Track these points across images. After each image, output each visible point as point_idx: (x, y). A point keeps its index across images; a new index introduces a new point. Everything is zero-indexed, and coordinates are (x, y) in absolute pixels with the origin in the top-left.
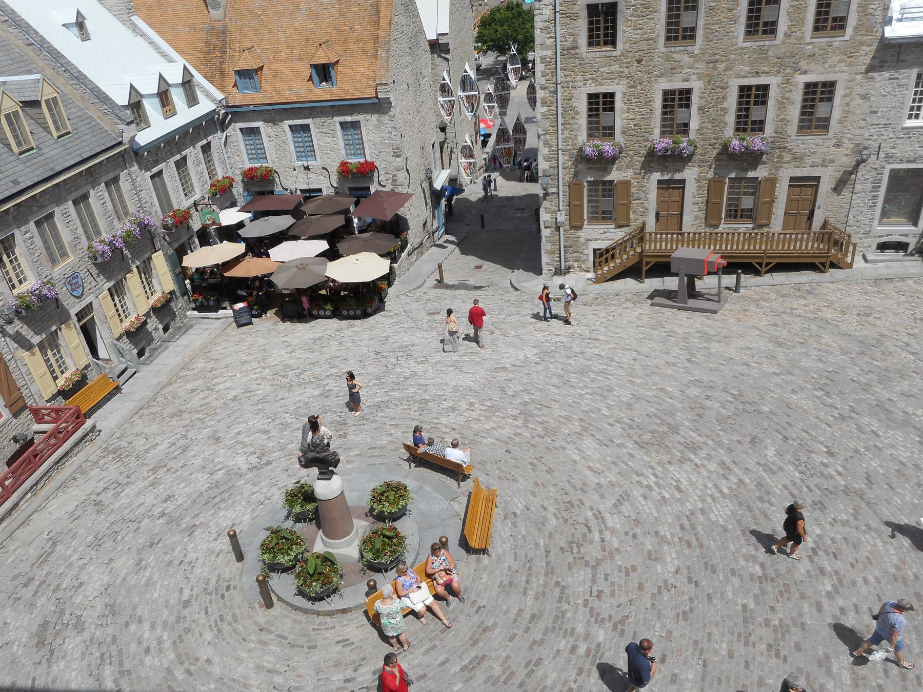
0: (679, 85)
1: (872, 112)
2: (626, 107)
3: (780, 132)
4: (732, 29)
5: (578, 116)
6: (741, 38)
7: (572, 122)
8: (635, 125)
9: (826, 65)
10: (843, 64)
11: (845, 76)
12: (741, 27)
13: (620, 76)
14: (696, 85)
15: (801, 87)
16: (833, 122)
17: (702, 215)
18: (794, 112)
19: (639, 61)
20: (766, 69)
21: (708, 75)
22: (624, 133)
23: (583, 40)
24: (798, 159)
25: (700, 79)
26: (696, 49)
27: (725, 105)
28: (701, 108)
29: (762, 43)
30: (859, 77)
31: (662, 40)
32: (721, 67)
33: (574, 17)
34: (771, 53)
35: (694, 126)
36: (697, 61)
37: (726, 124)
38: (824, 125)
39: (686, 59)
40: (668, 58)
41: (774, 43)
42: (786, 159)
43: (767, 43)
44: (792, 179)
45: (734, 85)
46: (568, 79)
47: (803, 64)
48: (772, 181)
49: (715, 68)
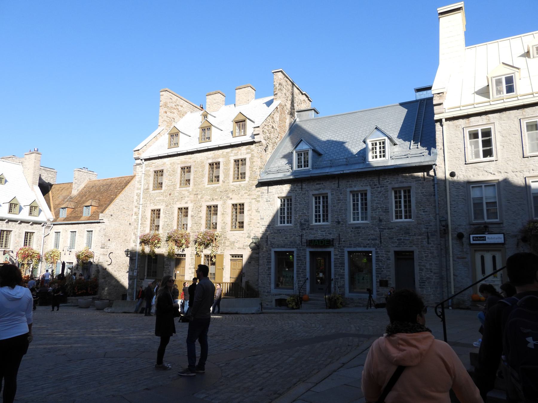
0: (183, 205)
1: (261, 219)
3: (223, 228)
6: (207, 183)
7: (144, 223)
8: (167, 225)
9: (240, 196)
10: (247, 195)
11: (249, 201)
12: (206, 179)
13: (163, 201)
14: (190, 206)
16: (245, 225)
18: (228, 219)
19: (170, 194)
20: (216, 197)
21: (195, 201)
22: (163, 228)
25: (191, 202)
29: (214, 185)
30: (254, 200)
32: (199, 197)
34: (218, 190)
35: (189, 226)
36: (190, 194)
38: (241, 225)
39: (186, 193)
40: (180, 193)
42: (227, 245)
43: (216, 185)
44: (233, 256)
47: (230, 195)
48: (222, 256)
49: (197, 197)
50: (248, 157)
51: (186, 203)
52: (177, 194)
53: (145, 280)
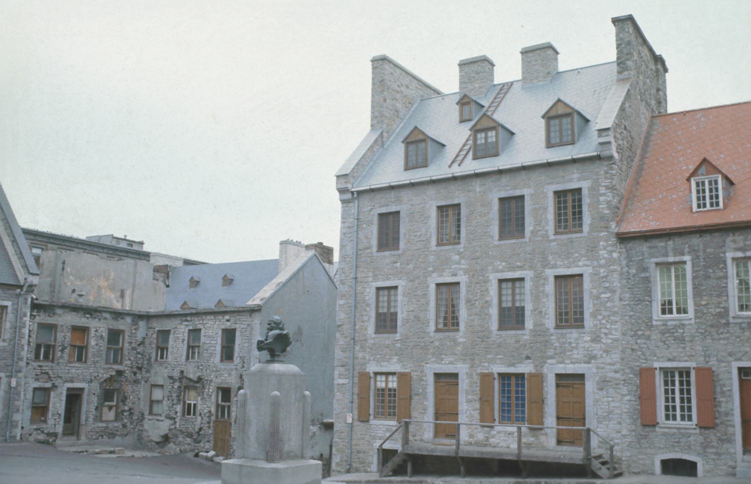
2: (406, 299)
4: (489, 230)
5: (368, 309)
12: (495, 230)
14: (462, 279)
15: (552, 279)
17: (476, 415)
23: (374, 242)
24: (562, 354)
26: (461, 247)
27: (488, 299)
28: (468, 301)
31: (434, 241)
33: (370, 223)
36: (463, 258)
37: (490, 316)
41: (524, 240)
45: (493, 278)
46: (363, 275)
48: (538, 378)
50: (585, 185)
51: (455, 275)
52: (432, 258)
53: (373, 422)
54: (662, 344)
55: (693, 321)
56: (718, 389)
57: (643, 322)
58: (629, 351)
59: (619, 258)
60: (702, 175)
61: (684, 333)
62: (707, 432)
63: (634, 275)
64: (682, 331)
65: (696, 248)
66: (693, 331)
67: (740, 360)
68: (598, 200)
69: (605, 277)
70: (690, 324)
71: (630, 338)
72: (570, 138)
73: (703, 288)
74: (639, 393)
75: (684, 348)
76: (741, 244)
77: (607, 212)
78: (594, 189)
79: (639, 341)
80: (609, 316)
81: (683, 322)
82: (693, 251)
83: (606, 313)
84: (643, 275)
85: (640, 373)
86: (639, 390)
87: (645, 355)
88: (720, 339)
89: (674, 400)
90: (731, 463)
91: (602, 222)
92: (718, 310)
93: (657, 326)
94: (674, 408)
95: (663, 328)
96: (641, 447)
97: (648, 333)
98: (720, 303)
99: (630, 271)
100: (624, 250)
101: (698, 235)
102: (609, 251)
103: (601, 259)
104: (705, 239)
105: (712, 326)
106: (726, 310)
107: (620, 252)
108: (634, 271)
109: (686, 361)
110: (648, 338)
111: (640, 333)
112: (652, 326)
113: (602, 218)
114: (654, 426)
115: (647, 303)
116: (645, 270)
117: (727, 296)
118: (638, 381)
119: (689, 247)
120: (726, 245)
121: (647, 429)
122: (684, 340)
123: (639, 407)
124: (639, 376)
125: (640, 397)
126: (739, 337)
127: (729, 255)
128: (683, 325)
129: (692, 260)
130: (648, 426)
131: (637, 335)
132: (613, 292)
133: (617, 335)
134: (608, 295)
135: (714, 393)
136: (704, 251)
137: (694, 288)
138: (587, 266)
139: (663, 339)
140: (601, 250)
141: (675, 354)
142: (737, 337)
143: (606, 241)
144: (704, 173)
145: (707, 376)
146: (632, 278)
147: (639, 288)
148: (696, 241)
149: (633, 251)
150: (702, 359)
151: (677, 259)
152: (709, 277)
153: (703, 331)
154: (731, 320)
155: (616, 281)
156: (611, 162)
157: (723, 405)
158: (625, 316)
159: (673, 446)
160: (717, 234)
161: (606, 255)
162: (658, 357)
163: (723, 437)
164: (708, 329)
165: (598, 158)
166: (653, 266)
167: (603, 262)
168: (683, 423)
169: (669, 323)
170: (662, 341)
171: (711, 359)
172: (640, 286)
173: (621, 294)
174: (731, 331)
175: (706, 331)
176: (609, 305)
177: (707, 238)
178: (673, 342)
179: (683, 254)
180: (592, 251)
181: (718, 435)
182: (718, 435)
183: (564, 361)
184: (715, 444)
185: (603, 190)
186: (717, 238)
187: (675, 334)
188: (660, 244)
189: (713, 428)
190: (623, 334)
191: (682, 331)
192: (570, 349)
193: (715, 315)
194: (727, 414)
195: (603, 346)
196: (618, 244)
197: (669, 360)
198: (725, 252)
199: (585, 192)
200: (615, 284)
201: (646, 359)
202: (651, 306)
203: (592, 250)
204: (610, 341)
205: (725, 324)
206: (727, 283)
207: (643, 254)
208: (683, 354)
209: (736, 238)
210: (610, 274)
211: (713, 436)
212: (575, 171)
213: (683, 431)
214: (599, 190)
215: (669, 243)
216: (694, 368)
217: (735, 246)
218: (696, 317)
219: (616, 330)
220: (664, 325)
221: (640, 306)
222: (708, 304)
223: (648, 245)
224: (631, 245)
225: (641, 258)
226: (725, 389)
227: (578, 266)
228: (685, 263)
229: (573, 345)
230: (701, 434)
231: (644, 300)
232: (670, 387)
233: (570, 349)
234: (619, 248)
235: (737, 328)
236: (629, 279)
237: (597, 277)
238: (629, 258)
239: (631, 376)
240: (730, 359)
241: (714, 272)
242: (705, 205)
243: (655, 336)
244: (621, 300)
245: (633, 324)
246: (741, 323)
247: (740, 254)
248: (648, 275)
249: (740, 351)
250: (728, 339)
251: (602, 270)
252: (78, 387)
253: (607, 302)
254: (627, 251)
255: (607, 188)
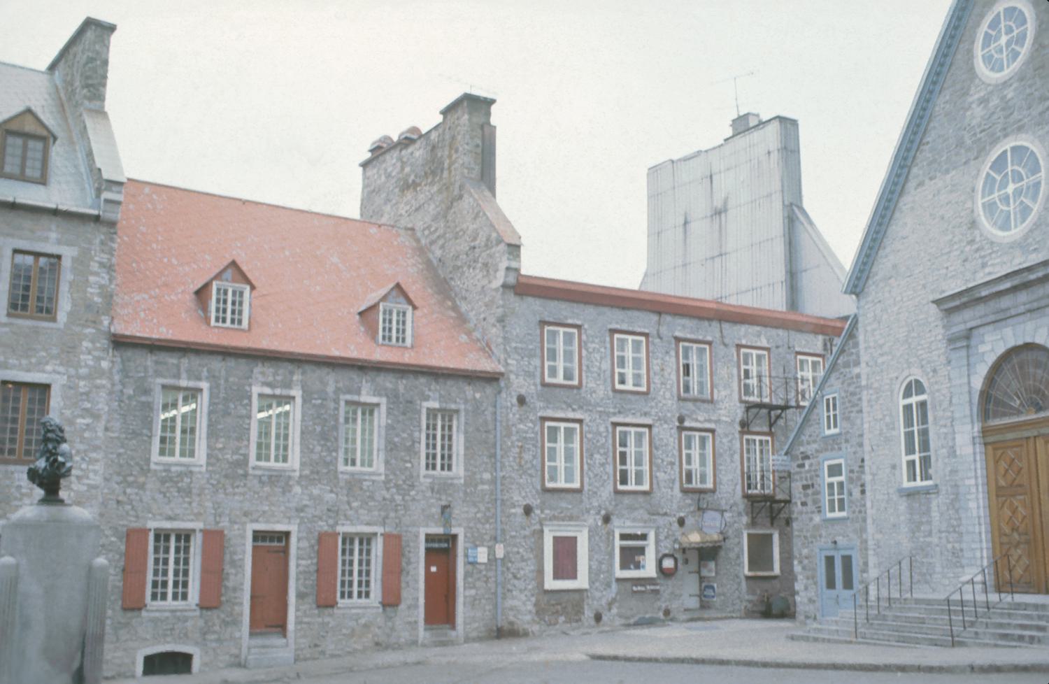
54: (161, 496)
55: (204, 469)
56: (227, 557)
57: (137, 464)
58: (113, 504)
59: (111, 369)
60: (227, 280)
61: (191, 482)
62: (209, 613)
63: (130, 398)
64: (189, 480)
65: (217, 374)
66: (204, 481)
67: (257, 521)
68: (87, 280)
69: (87, 394)
70: (200, 473)
71: (116, 486)
72: (37, 174)
73: (220, 427)
74: (122, 563)
75: (190, 503)
76: (271, 379)
77: (97, 299)
78: (81, 262)
79: (129, 491)
80: (85, 451)
81: (194, 469)
82: (212, 377)
83: (82, 447)
84: (143, 399)
85: (128, 535)
86: (123, 559)
87: (136, 511)
88: (234, 494)
89: (165, 573)
90: (234, 651)
91: (88, 312)
92: (235, 457)
93: (155, 471)
94: (165, 584)
95: (164, 474)
96: (118, 640)
97: (142, 479)
98: (239, 448)
99: (125, 391)
100: (119, 360)
101: (220, 358)
102: (93, 355)
103: (81, 367)
104: (229, 364)
105: (226, 476)
106: (246, 457)
107: (113, 362)
108: (131, 392)
109: (192, 520)
110: (142, 487)
111: (131, 479)
112: (149, 470)
113: (89, 307)
114: (140, 609)
115: (145, 438)
116: (147, 392)
117: (249, 440)
118: (123, 548)
119: (208, 371)
120: (254, 376)
121: (129, 614)
122: (190, 492)
123: (121, 584)
124: (124, 540)
125: (124, 570)
126: (258, 493)
127: (256, 390)
128: (191, 472)
129: (211, 389)
130: (132, 609)
131: (126, 481)
132: (96, 417)
133: (96, 479)
134: (88, 421)
135: (221, 561)
136: (227, 380)
137: (209, 426)
138: (59, 373)
139: (163, 490)
140: (84, 354)
141: (178, 511)
142: (255, 492)
143: (93, 342)
144: (230, 279)
145: (215, 541)
146: (127, 402)
147: (135, 416)
148: (217, 364)
149: (132, 364)
150: (211, 518)
151: (191, 384)
152: (229, 414)
153: (215, 482)
154: (251, 471)
155: (102, 403)
156: (112, 231)
157: (232, 577)
158: (112, 453)
159: (166, 635)
160: (243, 361)
161: (91, 363)
162: (154, 515)
163: (227, 619)
164: (223, 480)
165: (97, 219)
166: (158, 389)
167: (83, 371)
168: (176, 603)
169: (173, 469)
170: (161, 492)
171: (223, 519)
172: (137, 413)
173: (108, 421)
174: (249, 485)
175: (219, 482)
176: (87, 435)
177: (232, 363)
178: (176, 494)
179: (199, 379)
180: (68, 352)
181: (223, 616)
182: (223, 616)
183: (5, 514)
184: (217, 628)
185: (94, 267)
186: (354, 375)
187: (180, 485)
188: (172, 360)
189: (216, 608)
190: (106, 480)
191: (189, 480)
192: (18, 496)
193: (232, 463)
194: (235, 590)
195: (72, 494)
196: (111, 351)
197: (170, 518)
198: (250, 385)
199: (66, 263)
200: (100, 406)
201: (137, 517)
202: (150, 443)
203: (69, 351)
204: (85, 488)
205: (242, 475)
206: (249, 424)
207: (146, 368)
208: (188, 512)
209: (265, 369)
210: (94, 390)
211: (214, 615)
212: (53, 227)
213: (178, 614)
214: (89, 266)
215: (182, 360)
216: (201, 530)
217: (263, 380)
218: (208, 464)
219: (95, 472)
220: (165, 471)
221: (134, 442)
222: (224, 448)
223: (154, 358)
224: (129, 353)
225: (142, 374)
226: (236, 557)
227: (44, 371)
228: (201, 390)
229: (24, 491)
230: (201, 616)
231: (141, 434)
232: (161, 556)
233: (18, 496)
234: (111, 354)
235: (256, 481)
236: (122, 401)
237: (72, 391)
238: (125, 372)
239: (113, 539)
240: (244, 519)
241: (236, 408)
242: (224, 321)
243: (152, 484)
244: (107, 429)
245: (121, 466)
246: (260, 477)
247: (268, 391)
248: (150, 399)
249: (257, 511)
250: (243, 494)
251: (82, 383)
252: (579, 568)
253: (85, 430)
254: (123, 362)
255: (102, 265)
